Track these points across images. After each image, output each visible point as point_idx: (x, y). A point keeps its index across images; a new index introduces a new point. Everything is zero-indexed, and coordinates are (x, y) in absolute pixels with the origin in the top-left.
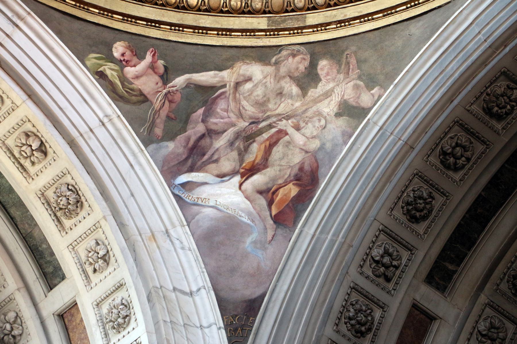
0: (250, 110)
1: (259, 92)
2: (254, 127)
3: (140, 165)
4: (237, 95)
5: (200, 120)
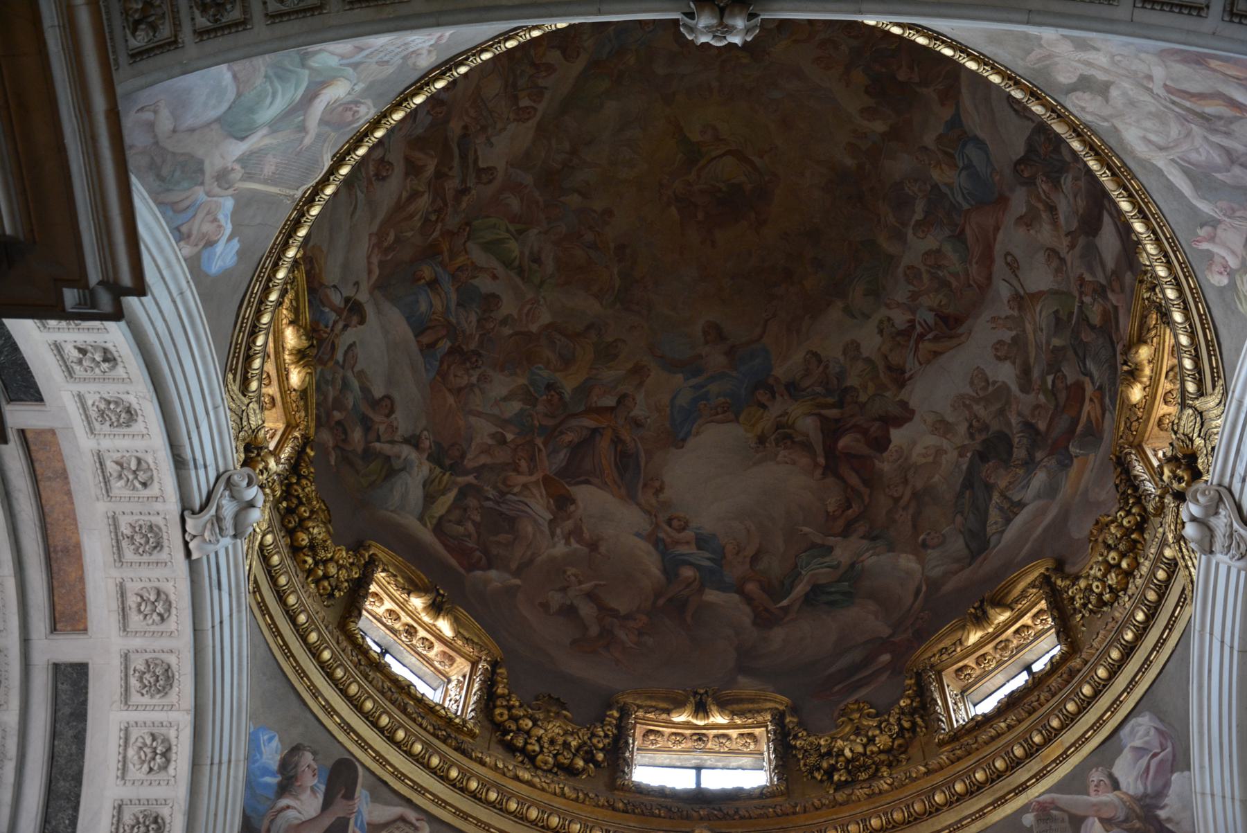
0: (1175, 130)
1: (1148, 124)
2: (1191, 117)
4: (1172, 145)
5: (1229, 174)
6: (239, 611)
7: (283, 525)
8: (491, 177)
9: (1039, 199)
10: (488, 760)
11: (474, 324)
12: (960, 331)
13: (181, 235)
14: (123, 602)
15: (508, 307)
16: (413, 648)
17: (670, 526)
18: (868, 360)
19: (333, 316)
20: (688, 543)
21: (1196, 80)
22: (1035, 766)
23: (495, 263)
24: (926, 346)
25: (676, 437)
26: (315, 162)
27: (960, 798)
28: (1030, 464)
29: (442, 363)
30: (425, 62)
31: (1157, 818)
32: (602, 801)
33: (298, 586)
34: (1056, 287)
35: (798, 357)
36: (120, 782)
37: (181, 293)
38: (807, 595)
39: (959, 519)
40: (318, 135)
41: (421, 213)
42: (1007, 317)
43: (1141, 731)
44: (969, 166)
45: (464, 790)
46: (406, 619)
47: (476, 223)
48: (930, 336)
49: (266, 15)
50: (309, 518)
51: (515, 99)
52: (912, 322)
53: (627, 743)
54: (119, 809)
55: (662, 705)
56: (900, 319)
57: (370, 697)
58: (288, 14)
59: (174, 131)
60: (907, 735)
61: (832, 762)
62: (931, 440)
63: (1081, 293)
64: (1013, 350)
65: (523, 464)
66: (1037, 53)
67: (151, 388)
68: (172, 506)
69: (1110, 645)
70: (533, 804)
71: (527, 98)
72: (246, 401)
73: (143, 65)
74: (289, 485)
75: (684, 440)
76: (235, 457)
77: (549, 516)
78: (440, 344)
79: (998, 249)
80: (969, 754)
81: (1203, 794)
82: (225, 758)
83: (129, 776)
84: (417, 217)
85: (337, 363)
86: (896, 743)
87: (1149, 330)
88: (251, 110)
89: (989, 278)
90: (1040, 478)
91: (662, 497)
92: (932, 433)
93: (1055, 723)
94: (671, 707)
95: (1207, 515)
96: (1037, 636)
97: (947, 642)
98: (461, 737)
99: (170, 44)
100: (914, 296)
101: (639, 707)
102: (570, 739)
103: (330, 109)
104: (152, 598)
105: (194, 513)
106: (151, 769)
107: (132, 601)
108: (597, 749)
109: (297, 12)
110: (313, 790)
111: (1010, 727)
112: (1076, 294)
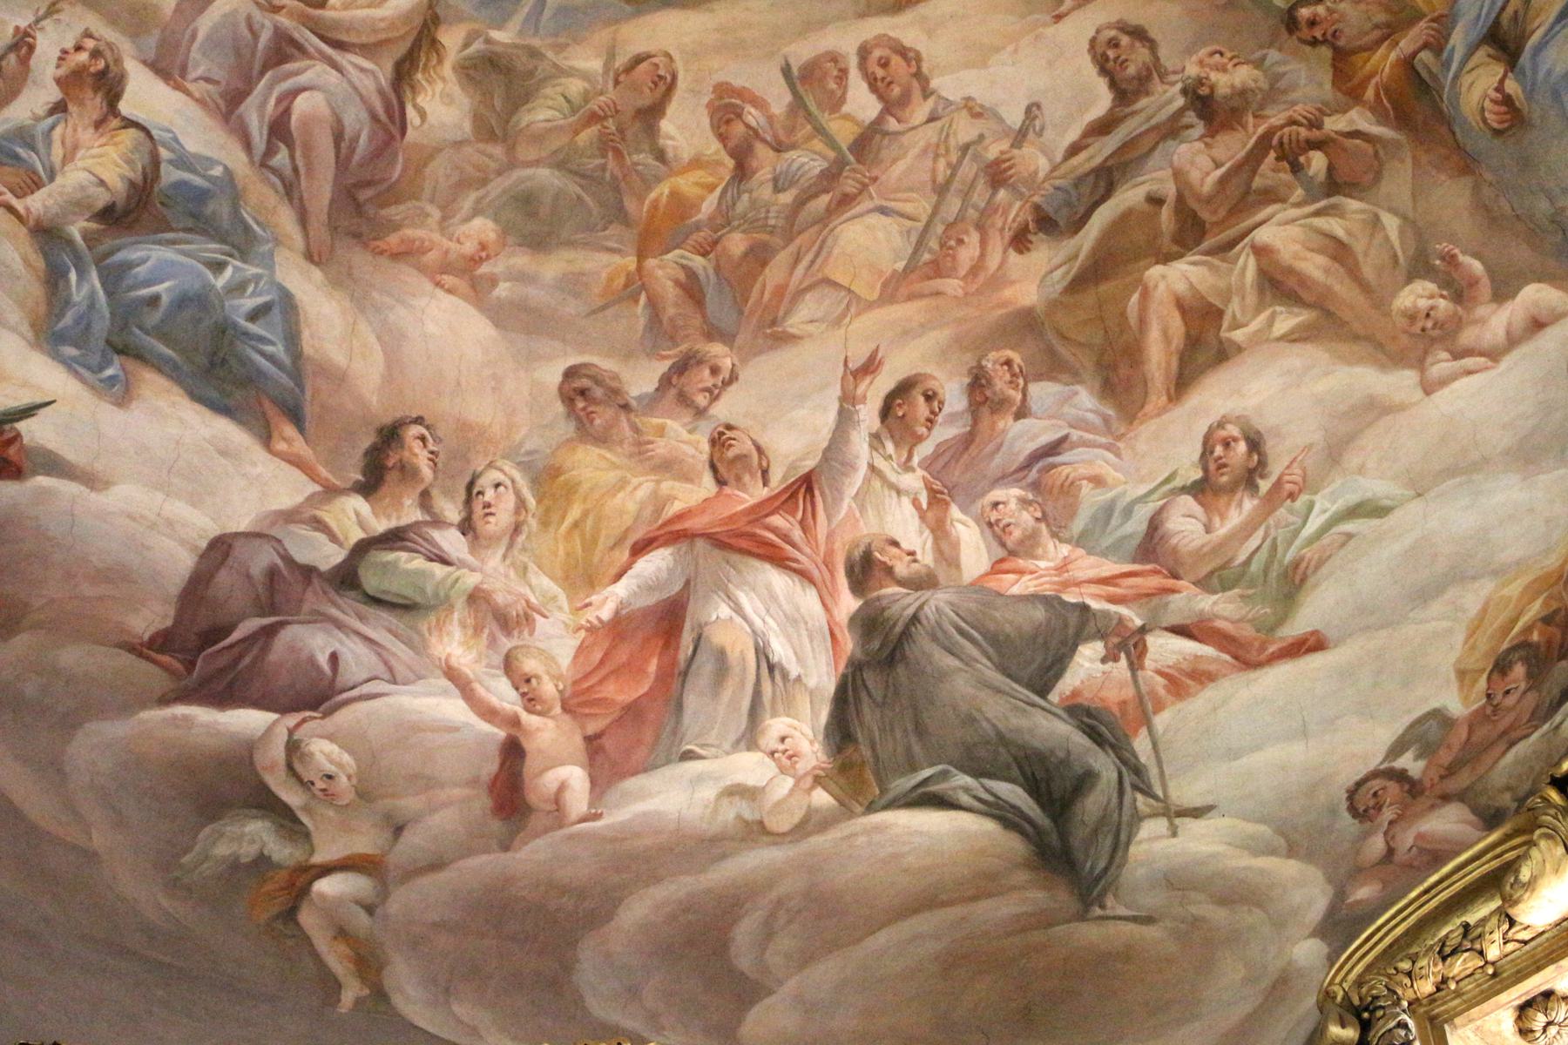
8: (1125, 40)
41: (1320, 222)
51: (867, 142)
71: (845, 109)
84: (1335, 226)
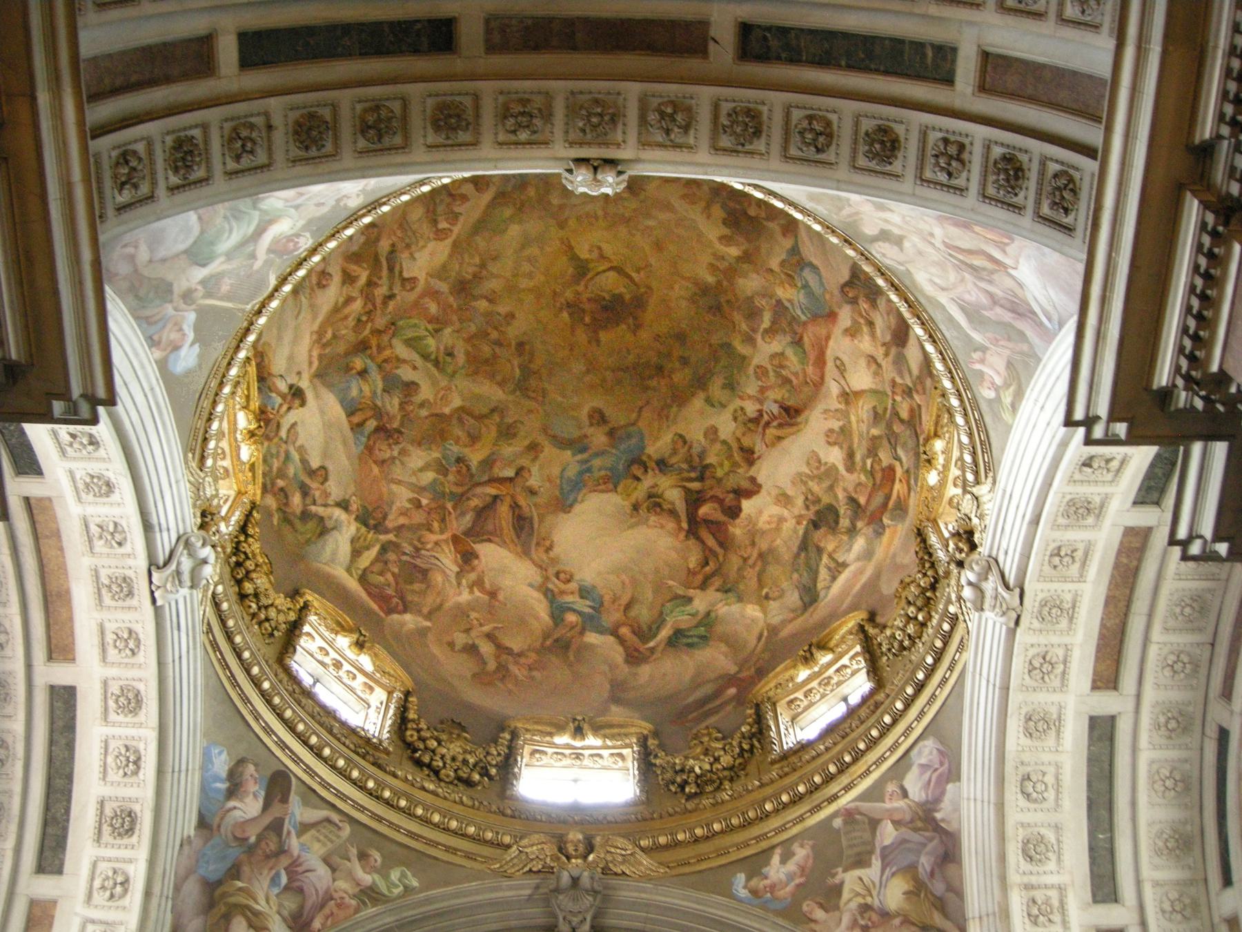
0: (952, 276)
1: (933, 270)
2: (963, 267)
3: (1053, 369)
6: (195, 648)
7: (233, 577)
9: (862, 316)
10: (399, 773)
11: (397, 406)
12: (799, 419)
13: (153, 342)
14: (103, 639)
15: (426, 392)
16: (339, 679)
17: (558, 578)
18: (724, 442)
19: (279, 400)
20: (572, 593)
21: (965, 240)
22: (844, 780)
23: (415, 357)
24: (771, 432)
25: (563, 504)
26: (263, 281)
27: (785, 806)
28: (852, 531)
29: (369, 438)
30: (354, 203)
31: (934, 819)
32: (494, 808)
33: (243, 628)
34: (874, 387)
35: (667, 438)
36: (102, 783)
37: (152, 389)
38: (670, 638)
39: (795, 576)
40: (266, 262)
42: (837, 410)
43: (926, 751)
44: (806, 286)
45: (378, 798)
46: (333, 655)
47: (401, 323)
48: (775, 423)
49: (226, 173)
50: (254, 571)
52: (760, 411)
53: (516, 760)
54: (102, 803)
55: (549, 729)
56: (751, 408)
57: (302, 720)
58: (243, 171)
59: (151, 261)
60: (746, 755)
61: (685, 777)
62: (776, 510)
63: (893, 393)
64: (841, 437)
65: (436, 525)
66: (846, 212)
67: (126, 466)
68: (142, 562)
69: (906, 683)
70: (437, 810)
72: (202, 475)
73: (126, 216)
74: (238, 543)
75: (571, 506)
76: (191, 521)
77: (456, 569)
78: (368, 423)
79: (829, 354)
80: (795, 770)
81: (968, 799)
82: (184, 767)
83: (109, 778)
85: (281, 439)
86: (738, 761)
87: (942, 427)
88: (212, 243)
89: (822, 378)
90: (860, 543)
91: (552, 554)
92: (775, 504)
93: (862, 746)
94: (553, 730)
95: (980, 580)
96: (853, 674)
97: (781, 679)
98: (377, 754)
99: (147, 199)
100: (762, 390)
101: (527, 730)
102: (468, 757)
103: (276, 241)
104: (126, 636)
105: (158, 568)
106: (125, 774)
107: (110, 638)
108: (491, 765)
109: (249, 170)
110: (255, 796)
111: (827, 749)
112: (890, 393)
